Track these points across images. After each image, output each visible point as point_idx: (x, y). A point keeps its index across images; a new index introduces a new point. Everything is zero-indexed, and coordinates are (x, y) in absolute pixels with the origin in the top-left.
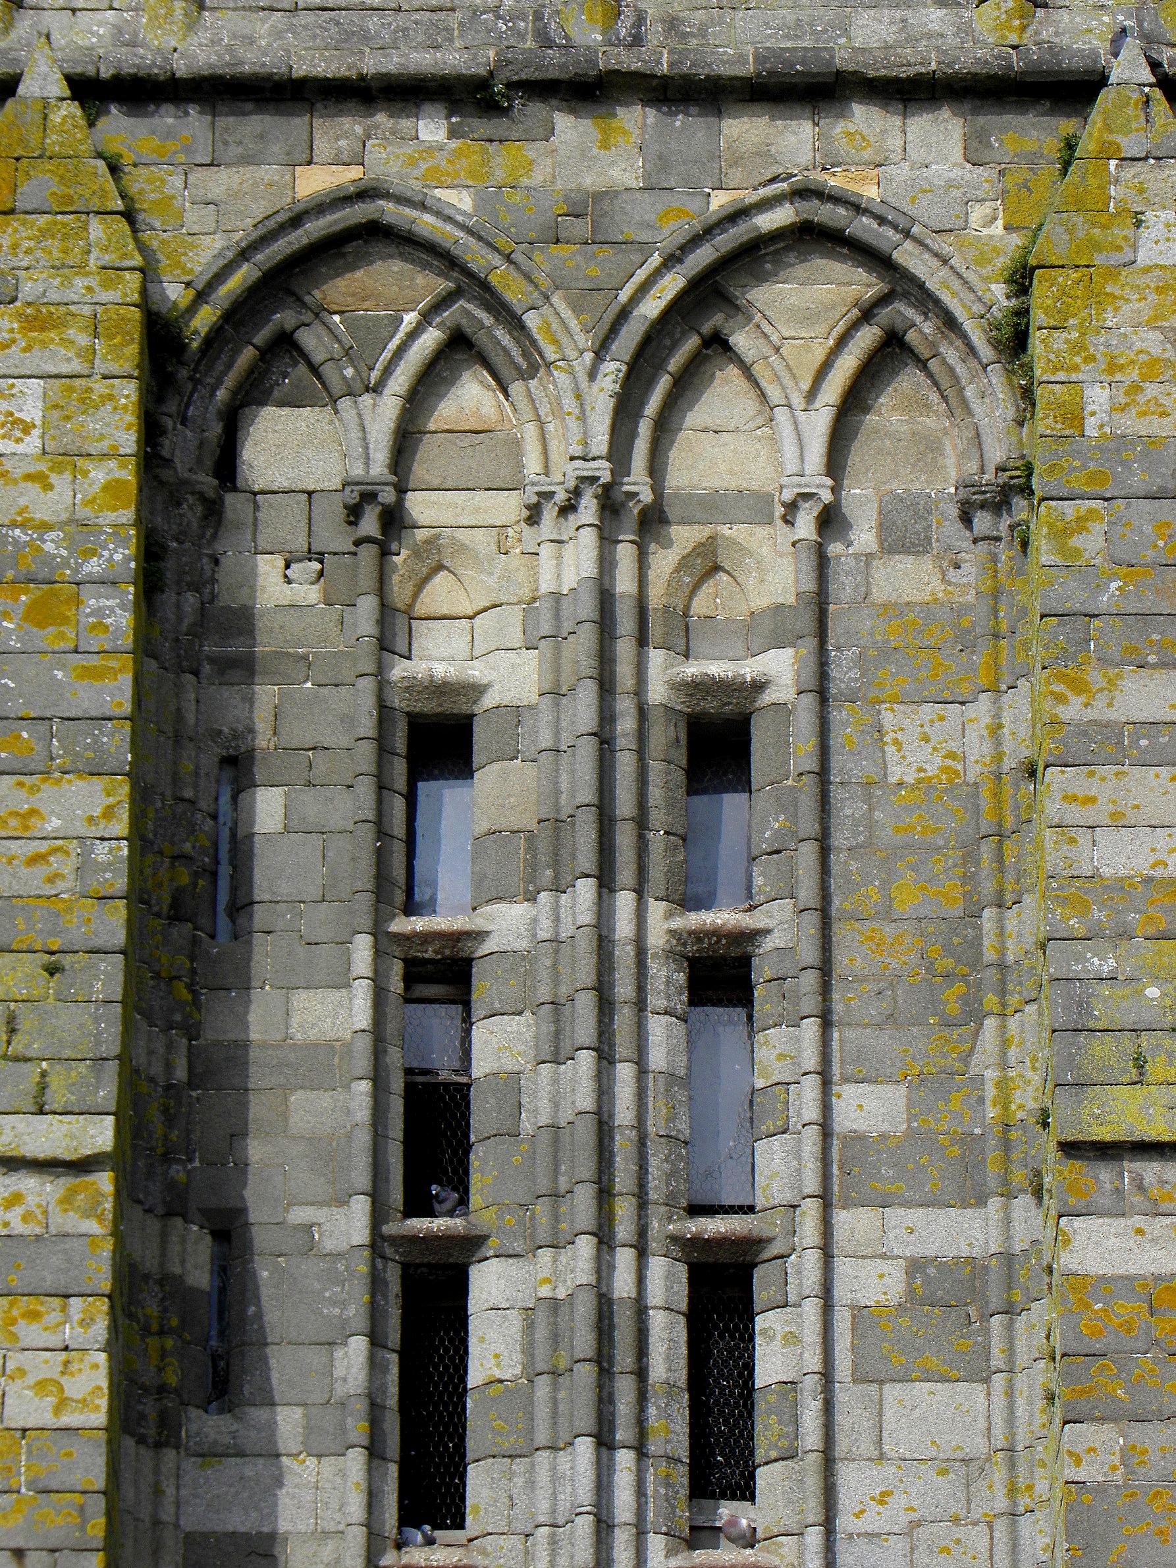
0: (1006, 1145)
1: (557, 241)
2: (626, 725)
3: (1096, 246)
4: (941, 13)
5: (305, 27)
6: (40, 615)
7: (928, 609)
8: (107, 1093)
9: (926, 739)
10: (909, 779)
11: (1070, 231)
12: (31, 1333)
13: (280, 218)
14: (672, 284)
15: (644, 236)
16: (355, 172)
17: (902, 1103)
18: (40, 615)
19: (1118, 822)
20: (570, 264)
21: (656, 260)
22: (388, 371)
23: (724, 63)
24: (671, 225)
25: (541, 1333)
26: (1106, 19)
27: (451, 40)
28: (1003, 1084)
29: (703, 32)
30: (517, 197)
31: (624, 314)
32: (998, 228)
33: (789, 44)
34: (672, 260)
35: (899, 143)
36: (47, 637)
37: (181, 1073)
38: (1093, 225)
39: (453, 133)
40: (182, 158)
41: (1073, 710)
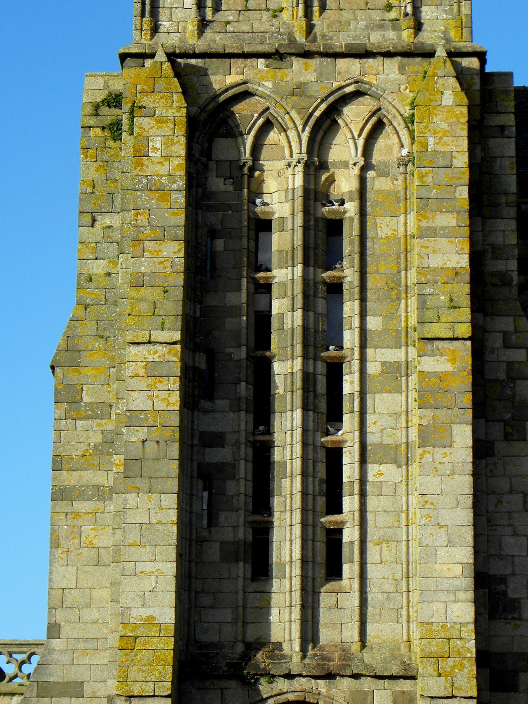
0: (407, 333)
1: (293, 95)
2: (312, 223)
3: (431, 101)
4: (393, 33)
5: (229, 37)
6: (162, 199)
7: (388, 192)
8: (179, 324)
9: (388, 226)
10: (383, 237)
11: (425, 96)
12: (160, 386)
13: (222, 90)
14: (323, 107)
15: (316, 94)
16: (242, 77)
17: (381, 322)
18: (162, 199)
19: (435, 253)
20: (297, 101)
21: (319, 100)
22: (250, 130)
23: (337, 48)
24: (323, 91)
25: (289, 381)
26: (436, 34)
27: (266, 41)
28: (407, 317)
29: (331, 38)
30: (283, 84)
31: (311, 115)
33: (354, 42)
34: (322, 101)
35: (382, 68)
36: (164, 205)
37: (198, 314)
38: (431, 95)
39: (267, 66)
40: (197, 73)
41: (424, 224)
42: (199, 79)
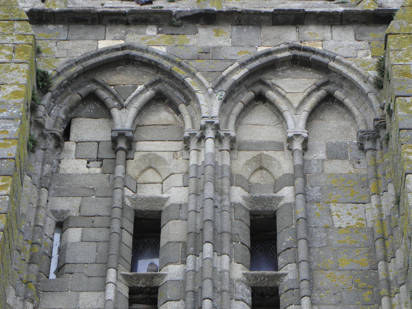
7: (348, 176)
9: (350, 214)
10: (344, 226)
14: (243, 72)
16: (122, 42)
21: (237, 64)
31: (223, 79)
32: (370, 57)
34: (243, 65)
39: (159, 32)
42: (58, 44)
